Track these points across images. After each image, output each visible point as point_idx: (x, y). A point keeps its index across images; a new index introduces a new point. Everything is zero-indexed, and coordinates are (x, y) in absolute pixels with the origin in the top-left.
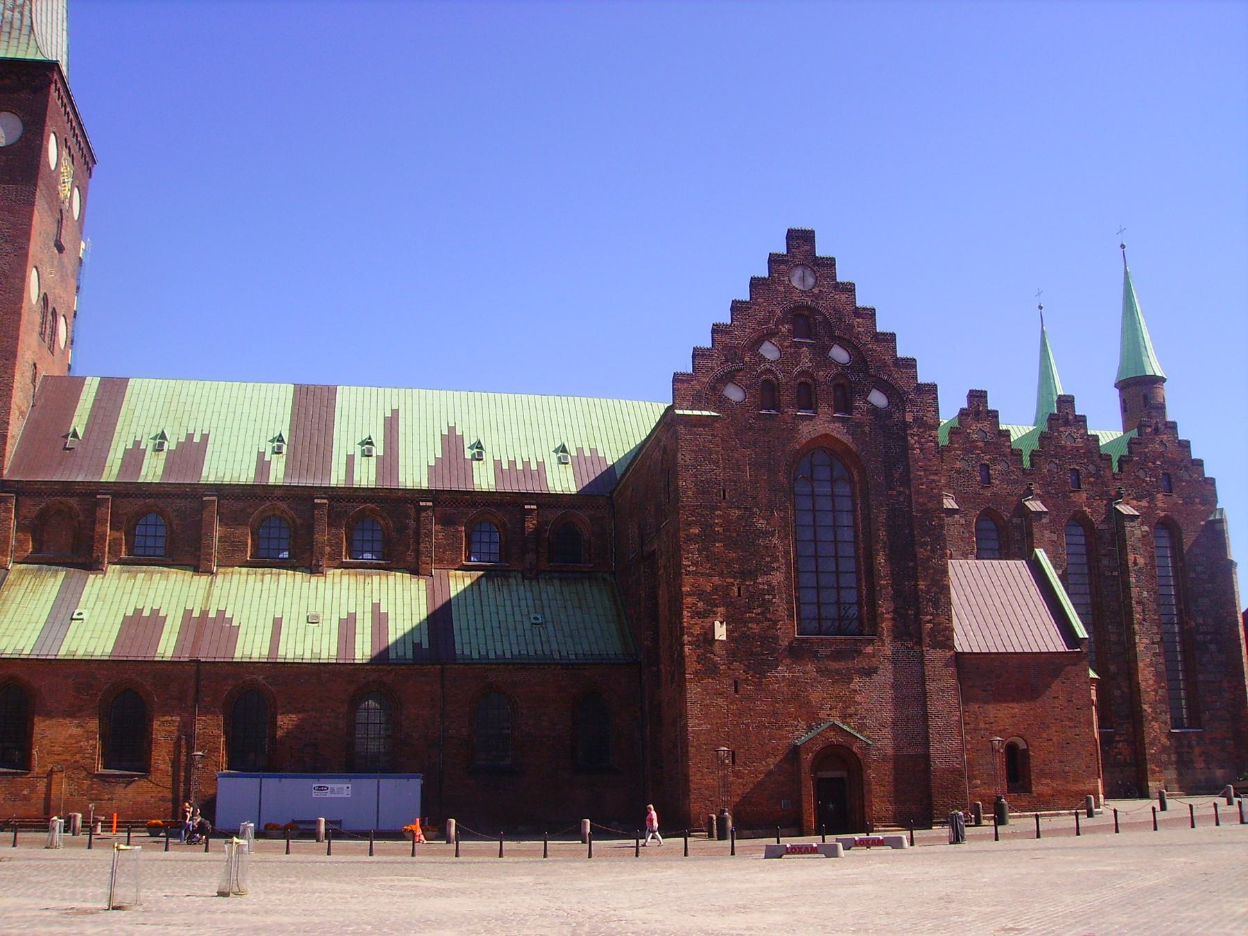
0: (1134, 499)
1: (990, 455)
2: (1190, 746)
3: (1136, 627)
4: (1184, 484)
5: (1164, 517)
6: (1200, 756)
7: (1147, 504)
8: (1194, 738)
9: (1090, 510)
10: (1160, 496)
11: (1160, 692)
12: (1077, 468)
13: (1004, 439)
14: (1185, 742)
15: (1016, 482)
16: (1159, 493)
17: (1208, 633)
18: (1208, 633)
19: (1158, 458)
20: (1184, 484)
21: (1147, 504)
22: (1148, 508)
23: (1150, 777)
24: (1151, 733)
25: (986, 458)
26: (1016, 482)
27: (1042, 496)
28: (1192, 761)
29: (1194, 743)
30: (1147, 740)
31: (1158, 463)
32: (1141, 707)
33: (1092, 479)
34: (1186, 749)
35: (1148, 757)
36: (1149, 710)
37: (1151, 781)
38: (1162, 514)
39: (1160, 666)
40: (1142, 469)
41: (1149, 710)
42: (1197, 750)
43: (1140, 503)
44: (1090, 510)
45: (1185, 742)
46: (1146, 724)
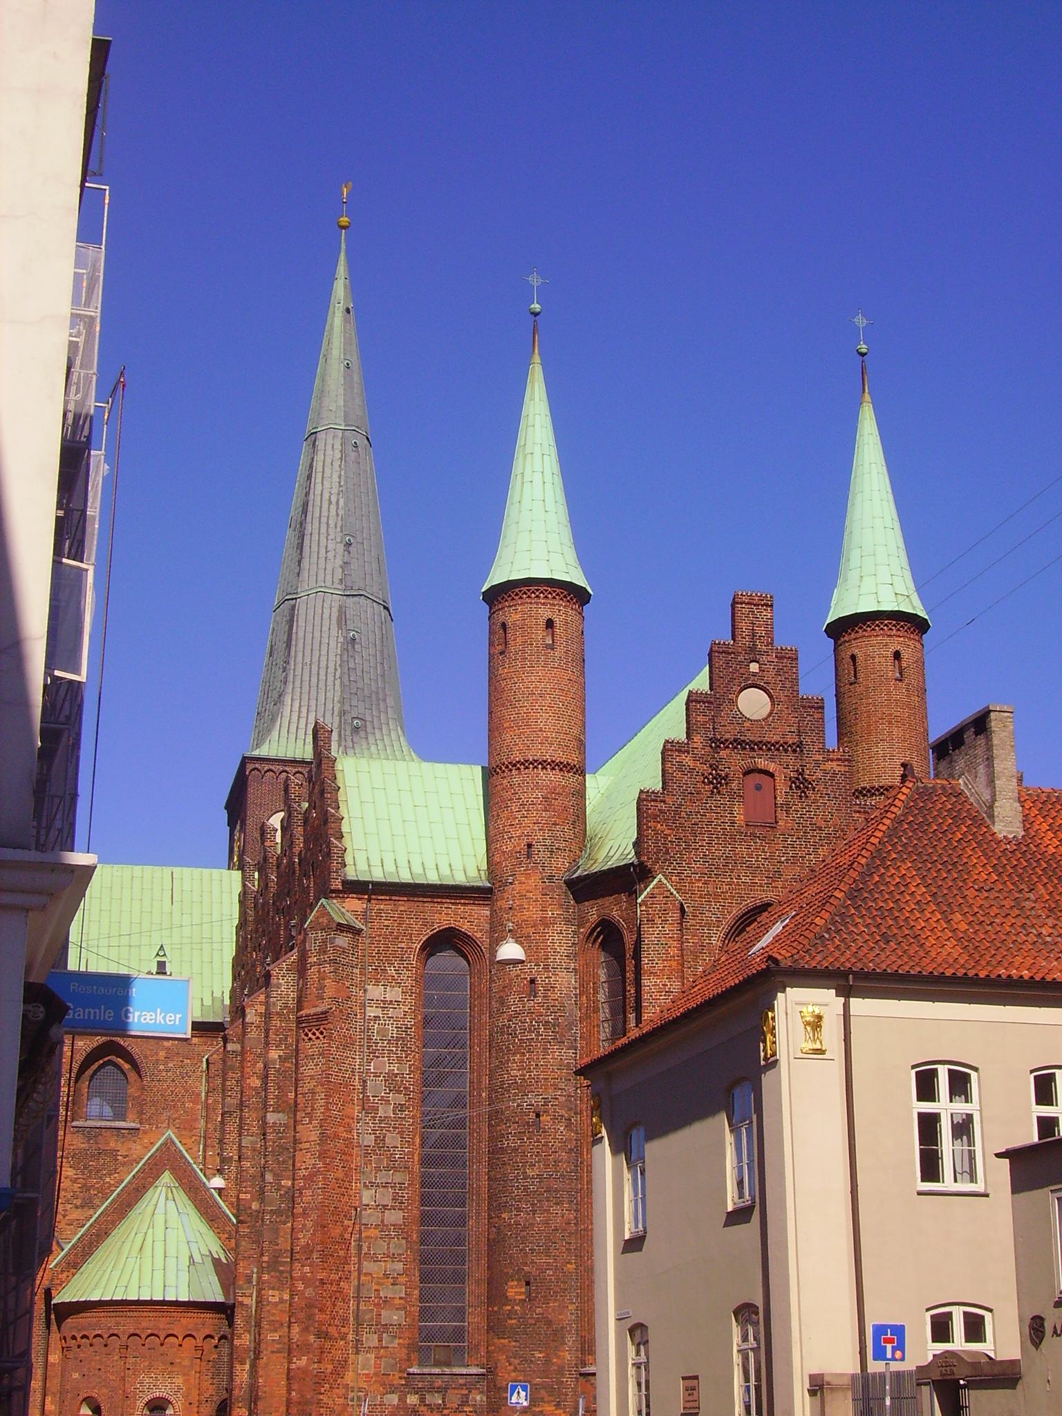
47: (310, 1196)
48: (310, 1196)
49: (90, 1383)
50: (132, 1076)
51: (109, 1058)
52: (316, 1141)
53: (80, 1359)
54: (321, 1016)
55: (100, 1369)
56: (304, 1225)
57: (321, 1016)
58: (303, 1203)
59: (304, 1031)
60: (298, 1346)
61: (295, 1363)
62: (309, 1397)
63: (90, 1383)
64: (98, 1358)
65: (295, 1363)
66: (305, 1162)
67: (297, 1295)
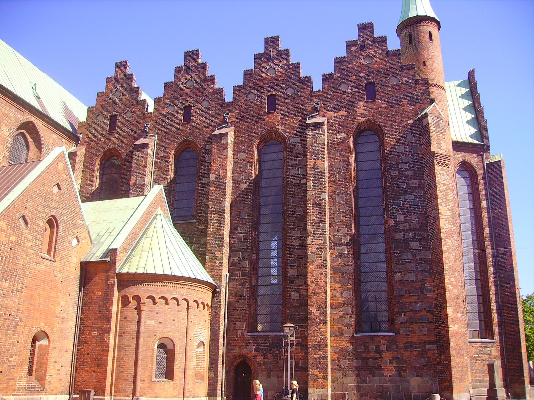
0: (331, 110)
1: (193, 98)
2: (378, 351)
3: (310, 228)
4: (390, 89)
5: (366, 121)
6: (391, 362)
7: (345, 113)
8: (383, 342)
9: (283, 127)
10: (361, 104)
11: (345, 294)
12: (274, 93)
13: (209, 83)
14: (372, 347)
15: (213, 115)
16: (360, 101)
17: (409, 230)
18: (409, 230)
19: (362, 71)
20: (390, 89)
21: (345, 113)
22: (347, 116)
23: (310, 383)
24: (317, 336)
25: (189, 102)
26: (213, 115)
27: (237, 123)
28: (379, 368)
29: (383, 348)
30: (311, 344)
31: (362, 74)
32: (307, 310)
33: (288, 101)
34: (372, 354)
35: (310, 362)
36: (317, 313)
37: (313, 387)
38: (363, 120)
39: (347, 267)
40: (345, 83)
41: (317, 313)
42: (387, 356)
43: (337, 114)
44: (283, 127)
45: (372, 347)
46: (312, 327)
47: (450, 243)
48: (450, 243)
49: (166, 328)
50: (32, 146)
51: (22, 131)
52: (450, 216)
53: (156, 312)
54: (447, 157)
55: (173, 320)
56: (449, 257)
57: (447, 157)
58: (447, 246)
59: (437, 161)
60: (452, 318)
61: (452, 327)
62: (461, 345)
63: (166, 328)
64: (173, 312)
65: (452, 327)
66: (445, 225)
67: (449, 292)
